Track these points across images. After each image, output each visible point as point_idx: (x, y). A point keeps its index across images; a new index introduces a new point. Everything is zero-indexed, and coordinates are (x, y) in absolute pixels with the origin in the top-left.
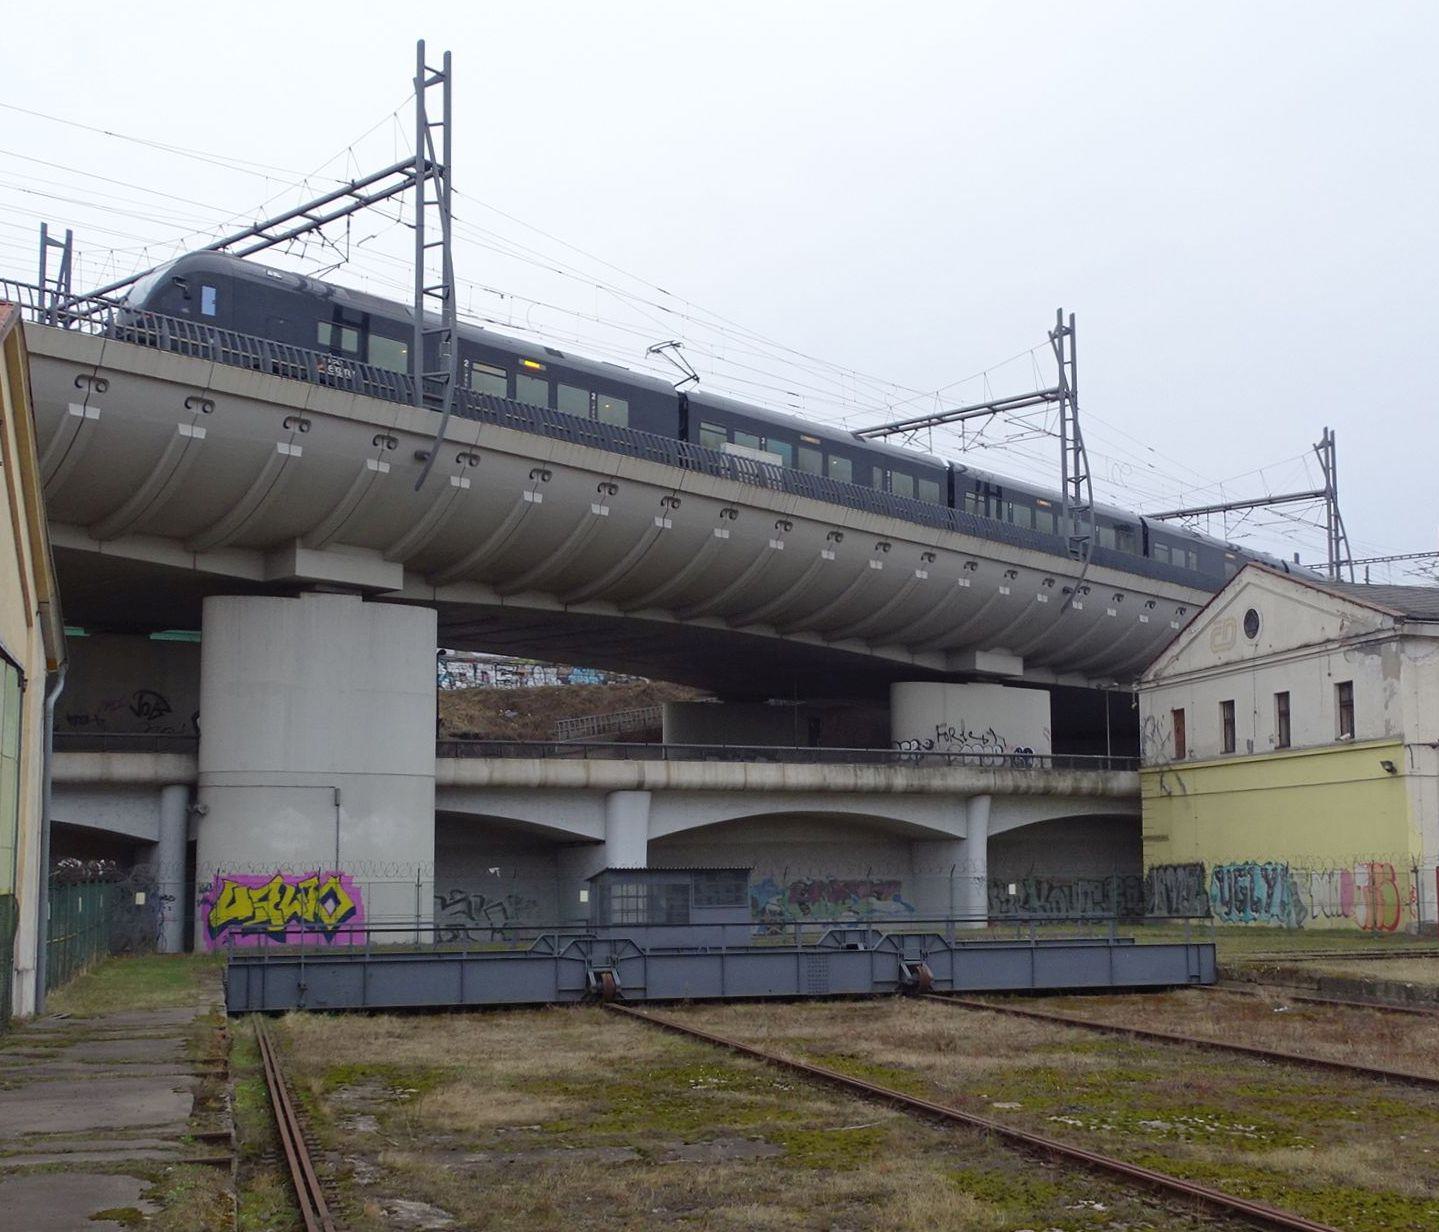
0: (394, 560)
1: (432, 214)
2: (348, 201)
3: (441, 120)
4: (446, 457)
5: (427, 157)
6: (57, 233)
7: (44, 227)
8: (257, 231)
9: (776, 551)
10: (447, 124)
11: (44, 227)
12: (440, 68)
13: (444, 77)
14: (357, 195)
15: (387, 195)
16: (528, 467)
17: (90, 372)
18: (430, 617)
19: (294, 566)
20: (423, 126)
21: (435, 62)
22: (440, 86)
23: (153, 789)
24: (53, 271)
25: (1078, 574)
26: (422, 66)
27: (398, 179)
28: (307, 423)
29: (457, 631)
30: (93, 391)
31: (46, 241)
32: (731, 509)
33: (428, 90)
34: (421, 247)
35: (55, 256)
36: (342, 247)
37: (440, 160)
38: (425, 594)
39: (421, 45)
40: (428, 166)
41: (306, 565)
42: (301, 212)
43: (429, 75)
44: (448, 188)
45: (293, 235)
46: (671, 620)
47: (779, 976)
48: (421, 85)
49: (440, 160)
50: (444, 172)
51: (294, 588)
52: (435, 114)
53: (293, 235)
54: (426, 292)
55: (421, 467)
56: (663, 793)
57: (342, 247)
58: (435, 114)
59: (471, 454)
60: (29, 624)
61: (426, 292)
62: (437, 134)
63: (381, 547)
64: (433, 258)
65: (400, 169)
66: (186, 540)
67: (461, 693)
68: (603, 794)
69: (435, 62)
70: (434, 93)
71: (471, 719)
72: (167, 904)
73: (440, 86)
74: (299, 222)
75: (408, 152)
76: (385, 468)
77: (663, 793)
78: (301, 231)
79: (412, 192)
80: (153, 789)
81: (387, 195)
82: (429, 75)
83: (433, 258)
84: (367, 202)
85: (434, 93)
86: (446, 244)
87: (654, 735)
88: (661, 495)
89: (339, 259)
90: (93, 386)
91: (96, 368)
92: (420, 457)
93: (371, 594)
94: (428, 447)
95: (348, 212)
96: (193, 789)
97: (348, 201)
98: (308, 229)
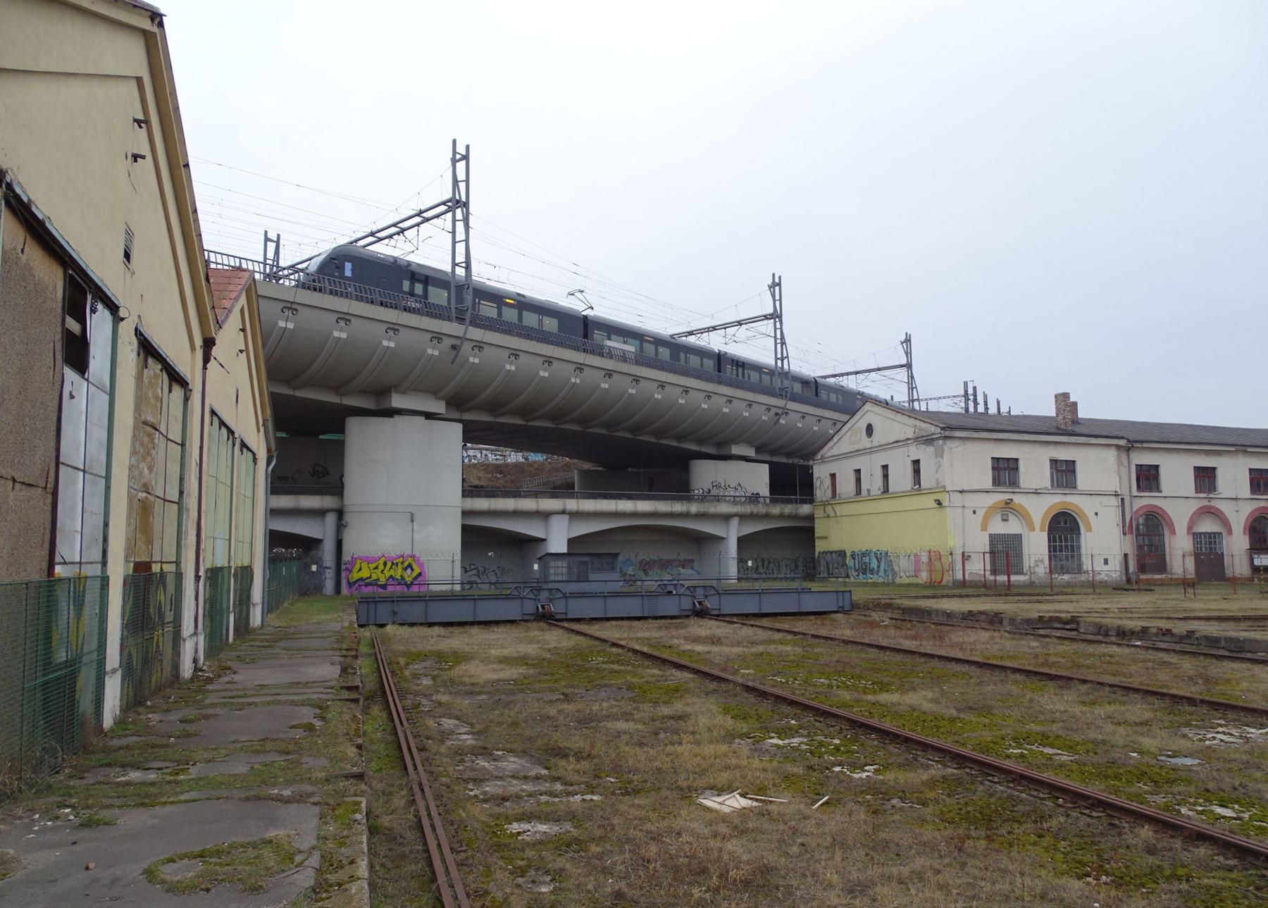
0: (441, 399)
1: (460, 226)
2: (418, 219)
3: (464, 179)
4: (467, 347)
5: (457, 197)
6: (272, 236)
7: (266, 232)
8: (372, 234)
9: (604, 388)
10: (467, 181)
11: (266, 232)
12: (464, 153)
13: (466, 158)
14: (422, 217)
15: (437, 216)
16: (384, 327)
17: (289, 305)
18: (458, 428)
19: (391, 402)
20: (455, 182)
21: (461, 150)
22: (464, 162)
23: (320, 513)
24: (271, 255)
25: (461, 335)
26: (455, 152)
27: (443, 208)
28: (397, 330)
29: (472, 434)
30: (290, 314)
31: (267, 239)
32: (609, 374)
33: (458, 164)
34: (454, 242)
35: (271, 247)
36: (415, 243)
37: (464, 199)
38: (457, 416)
39: (454, 142)
40: (458, 202)
41: (397, 401)
42: (395, 225)
43: (458, 157)
44: (468, 213)
45: (391, 237)
46: (579, 428)
47: (632, 606)
48: (454, 162)
49: (464, 199)
50: (466, 205)
51: (391, 413)
52: (461, 175)
53: (391, 237)
54: (457, 265)
55: (455, 352)
56: (575, 515)
57: (415, 242)
58: (461, 175)
59: (479, 346)
60: (258, 431)
61: (457, 265)
62: (462, 186)
63: (435, 392)
64: (460, 248)
65: (444, 203)
66: (337, 389)
67: (474, 465)
68: (545, 516)
69: (461, 150)
70: (461, 166)
71: (479, 478)
72: (327, 571)
73: (464, 162)
74: (394, 230)
75: (449, 195)
76: (436, 353)
77: (575, 515)
78: (394, 235)
79: (449, 215)
80: (320, 513)
81: (437, 216)
82: (458, 157)
83: (460, 248)
84: (428, 220)
85: (461, 166)
86: (467, 241)
87: (571, 486)
88: (574, 366)
89: (414, 249)
90: (290, 312)
91: (292, 303)
92: (454, 347)
93: (429, 416)
94: (457, 342)
95: (418, 225)
96: (340, 513)
97: (418, 219)
98: (398, 234)
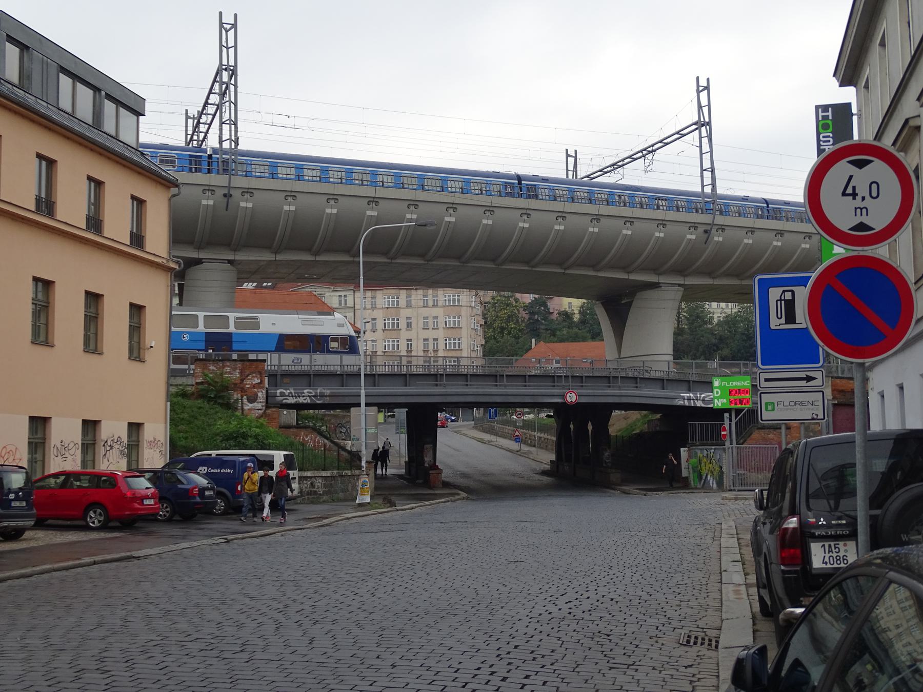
1: (705, 141)
7: (567, 150)
10: (709, 105)
11: (567, 150)
12: (706, 85)
13: (707, 88)
20: (700, 107)
21: (703, 83)
22: (706, 91)
24: (571, 167)
26: (698, 86)
27: (694, 127)
31: (568, 156)
34: (701, 154)
35: (571, 160)
39: (698, 78)
43: (701, 88)
49: (707, 120)
52: (704, 102)
58: (704, 102)
62: (705, 110)
64: (706, 157)
69: (703, 83)
73: (706, 91)
75: (696, 119)
82: (701, 88)
83: (706, 157)
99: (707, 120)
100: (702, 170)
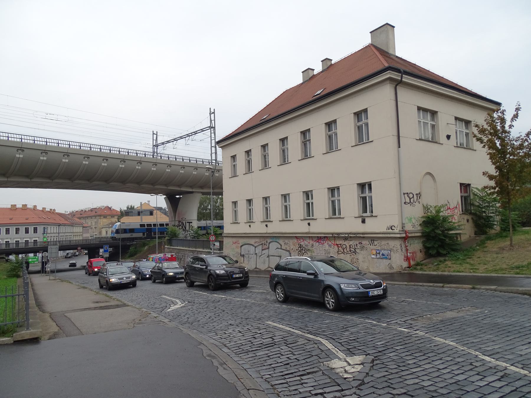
1: (213, 135)
5: (212, 126)
10: (214, 120)
12: (213, 112)
13: (214, 113)
20: (211, 121)
33: (211, 115)
34: (211, 140)
39: (210, 108)
43: (211, 113)
44: (215, 129)
48: (210, 114)
49: (214, 126)
50: (214, 128)
52: (213, 119)
58: (213, 119)
62: (213, 122)
66: (179, 186)
70: (212, 115)
85: (212, 115)
92: (212, 172)
94: (214, 170)
99: (214, 126)
100: (212, 147)
